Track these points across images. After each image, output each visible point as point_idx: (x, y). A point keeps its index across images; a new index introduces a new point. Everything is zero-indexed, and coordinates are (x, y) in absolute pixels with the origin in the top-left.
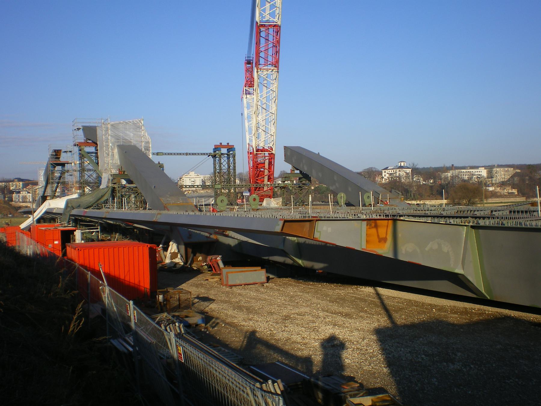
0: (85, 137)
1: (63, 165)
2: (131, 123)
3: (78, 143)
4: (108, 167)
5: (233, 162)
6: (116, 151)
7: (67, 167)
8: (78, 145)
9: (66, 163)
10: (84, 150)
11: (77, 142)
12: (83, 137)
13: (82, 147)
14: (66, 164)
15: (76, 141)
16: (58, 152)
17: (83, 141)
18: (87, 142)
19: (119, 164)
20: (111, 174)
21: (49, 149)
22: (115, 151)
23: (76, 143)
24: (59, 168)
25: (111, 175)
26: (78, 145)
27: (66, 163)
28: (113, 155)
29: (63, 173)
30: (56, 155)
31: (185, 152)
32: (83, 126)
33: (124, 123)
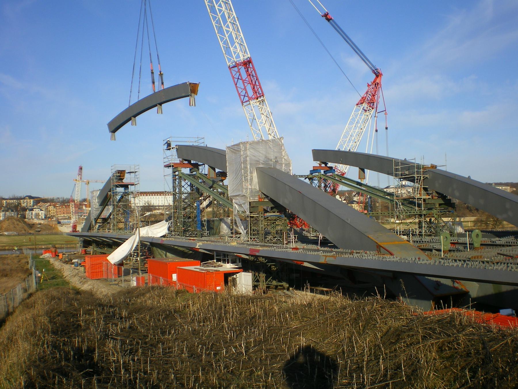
0: (179, 157)
1: (126, 186)
2: (271, 142)
3: (173, 164)
4: (247, 194)
5: (318, 185)
6: (255, 174)
7: (131, 188)
8: (173, 166)
9: (129, 185)
10: (182, 172)
11: (173, 163)
12: (176, 157)
13: (179, 169)
14: (129, 186)
15: (171, 162)
16: (121, 173)
17: (178, 162)
18: (184, 163)
19: (258, 189)
20: (250, 201)
21: (112, 170)
22: (253, 175)
23: (171, 164)
24: (121, 190)
25: (250, 202)
26: (173, 166)
27: (129, 185)
28: (251, 180)
29: (126, 194)
30: (120, 176)
31: (307, 175)
32: (176, 146)
33: (263, 142)
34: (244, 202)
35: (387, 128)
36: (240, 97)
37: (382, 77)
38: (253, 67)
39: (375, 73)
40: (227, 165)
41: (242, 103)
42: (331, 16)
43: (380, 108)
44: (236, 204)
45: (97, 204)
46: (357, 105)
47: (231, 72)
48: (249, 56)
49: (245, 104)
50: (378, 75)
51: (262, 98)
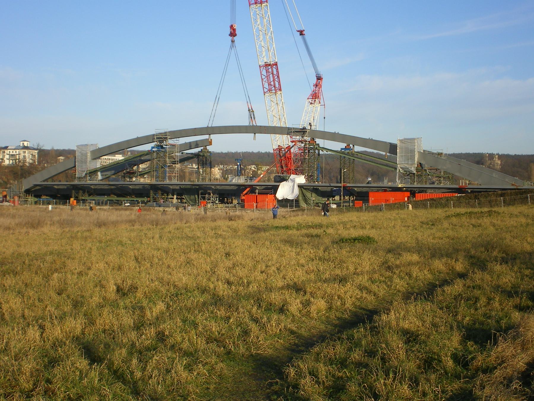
34: (410, 167)
35: (324, 118)
36: (263, 89)
37: (323, 80)
38: (277, 69)
39: (317, 77)
40: (398, 148)
41: (265, 93)
42: (304, 32)
43: (322, 103)
44: (401, 167)
45: (90, 157)
46: (308, 99)
47: (260, 70)
48: (276, 61)
49: (266, 94)
50: (319, 78)
51: (279, 92)
